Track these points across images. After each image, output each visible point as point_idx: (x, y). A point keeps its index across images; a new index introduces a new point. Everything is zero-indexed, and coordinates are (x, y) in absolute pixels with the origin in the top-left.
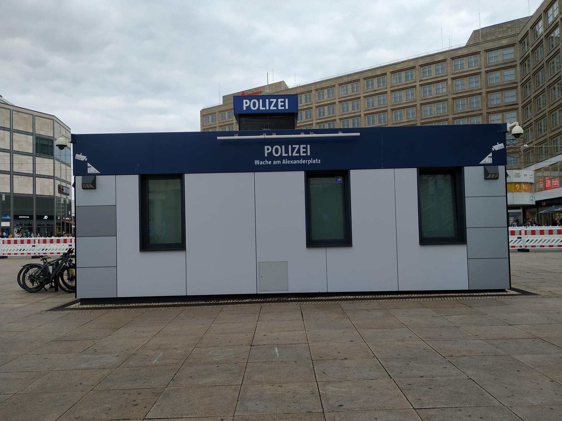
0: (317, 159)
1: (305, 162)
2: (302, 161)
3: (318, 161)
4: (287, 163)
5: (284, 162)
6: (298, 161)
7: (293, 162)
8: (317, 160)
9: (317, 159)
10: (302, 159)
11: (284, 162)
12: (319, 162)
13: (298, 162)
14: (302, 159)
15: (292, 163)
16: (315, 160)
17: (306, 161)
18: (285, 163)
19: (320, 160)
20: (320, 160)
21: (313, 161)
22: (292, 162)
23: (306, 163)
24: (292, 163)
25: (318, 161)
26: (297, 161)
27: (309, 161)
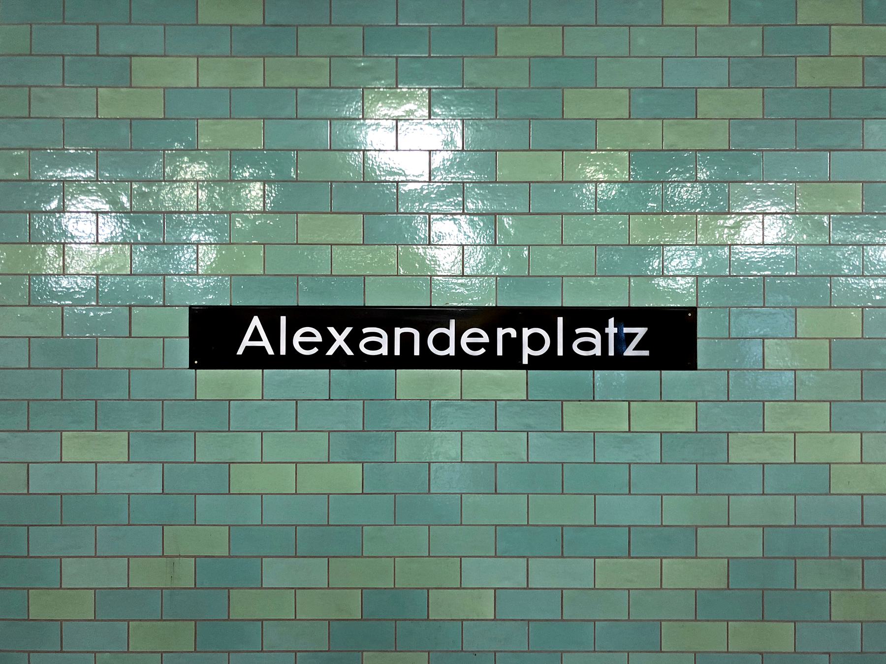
0: (611, 321)
1: (491, 346)
2: (451, 332)
3: (623, 340)
4: (283, 351)
5: (256, 336)
6: (417, 334)
7: (352, 341)
8: (611, 330)
9: (611, 321)
10: (452, 323)
11: (256, 336)
12: (629, 352)
13: (407, 339)
14: (452, 323)
15: (349, 352)
16: (601, 327)
17: (501, 332)
18: (270, 352)
19: (641, 331)
20: (641, 331)
21: (570, 337)
22: (340, 340)
23: (500, 352)
24: (349, 352)
25: (623, 340)
26: (398, 331)
27: (527, 332)
